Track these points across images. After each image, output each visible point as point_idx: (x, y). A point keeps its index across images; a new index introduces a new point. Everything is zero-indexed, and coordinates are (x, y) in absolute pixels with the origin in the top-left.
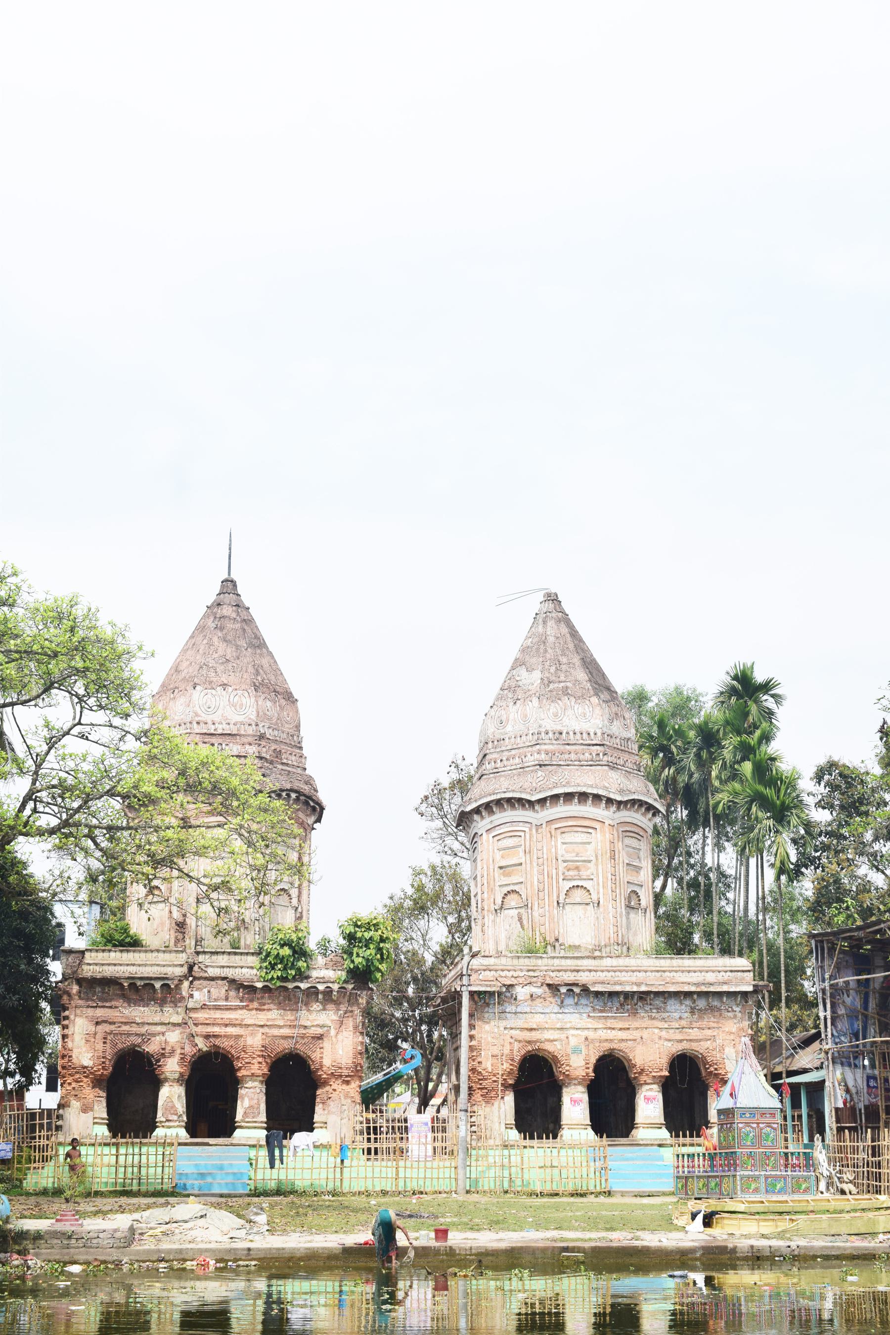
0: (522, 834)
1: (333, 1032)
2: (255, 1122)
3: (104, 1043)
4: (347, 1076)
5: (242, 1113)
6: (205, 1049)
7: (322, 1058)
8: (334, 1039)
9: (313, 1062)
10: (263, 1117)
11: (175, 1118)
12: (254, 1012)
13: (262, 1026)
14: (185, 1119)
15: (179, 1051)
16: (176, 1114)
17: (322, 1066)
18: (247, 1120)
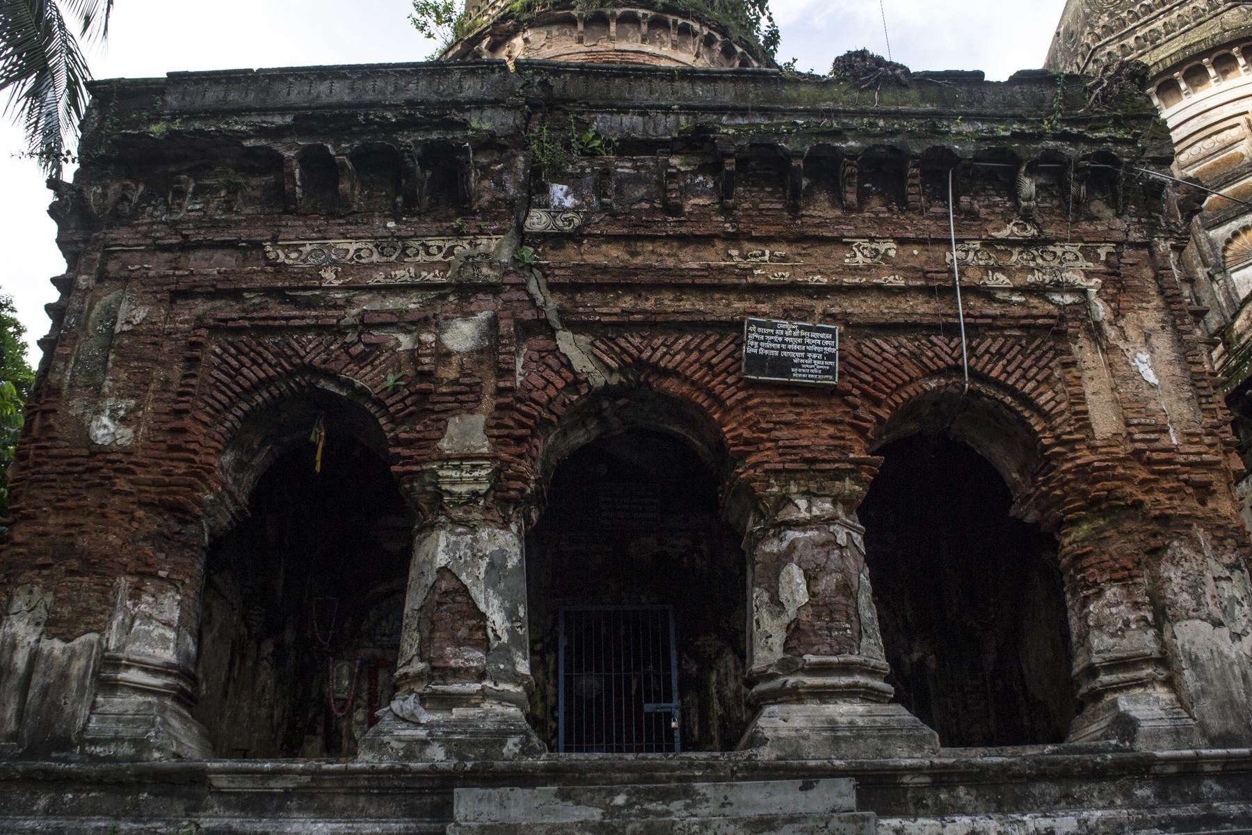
0: (1241, 119)
1: (1101, 310)
2: (846, 669)
3: (192, 362)
4: (1193, 465)
5: (778, 639)
6: (599, 380)
7: (1080, 398)
8: (1111, 333)
9: (1046, 416)
10: (872, 650)
11: (475, 658)
12: (782, 250)
13: (821, 292)
14: (523, 667)
15: (490, 384)
16: (484, 644)
17: (1083, 421)
18: (811, 658)
